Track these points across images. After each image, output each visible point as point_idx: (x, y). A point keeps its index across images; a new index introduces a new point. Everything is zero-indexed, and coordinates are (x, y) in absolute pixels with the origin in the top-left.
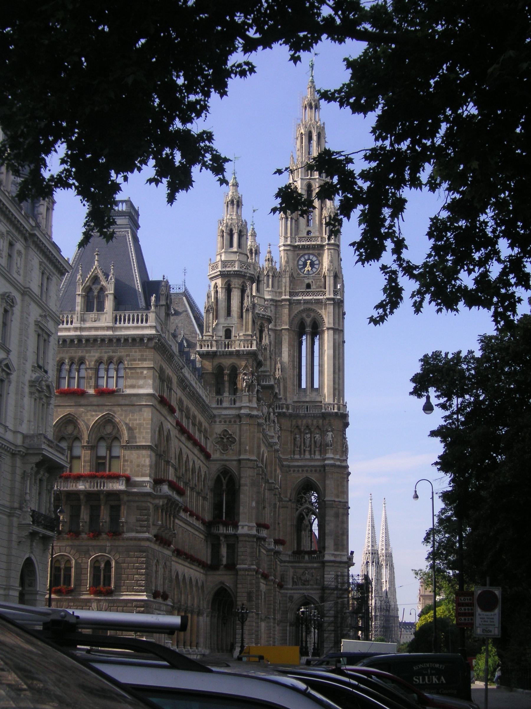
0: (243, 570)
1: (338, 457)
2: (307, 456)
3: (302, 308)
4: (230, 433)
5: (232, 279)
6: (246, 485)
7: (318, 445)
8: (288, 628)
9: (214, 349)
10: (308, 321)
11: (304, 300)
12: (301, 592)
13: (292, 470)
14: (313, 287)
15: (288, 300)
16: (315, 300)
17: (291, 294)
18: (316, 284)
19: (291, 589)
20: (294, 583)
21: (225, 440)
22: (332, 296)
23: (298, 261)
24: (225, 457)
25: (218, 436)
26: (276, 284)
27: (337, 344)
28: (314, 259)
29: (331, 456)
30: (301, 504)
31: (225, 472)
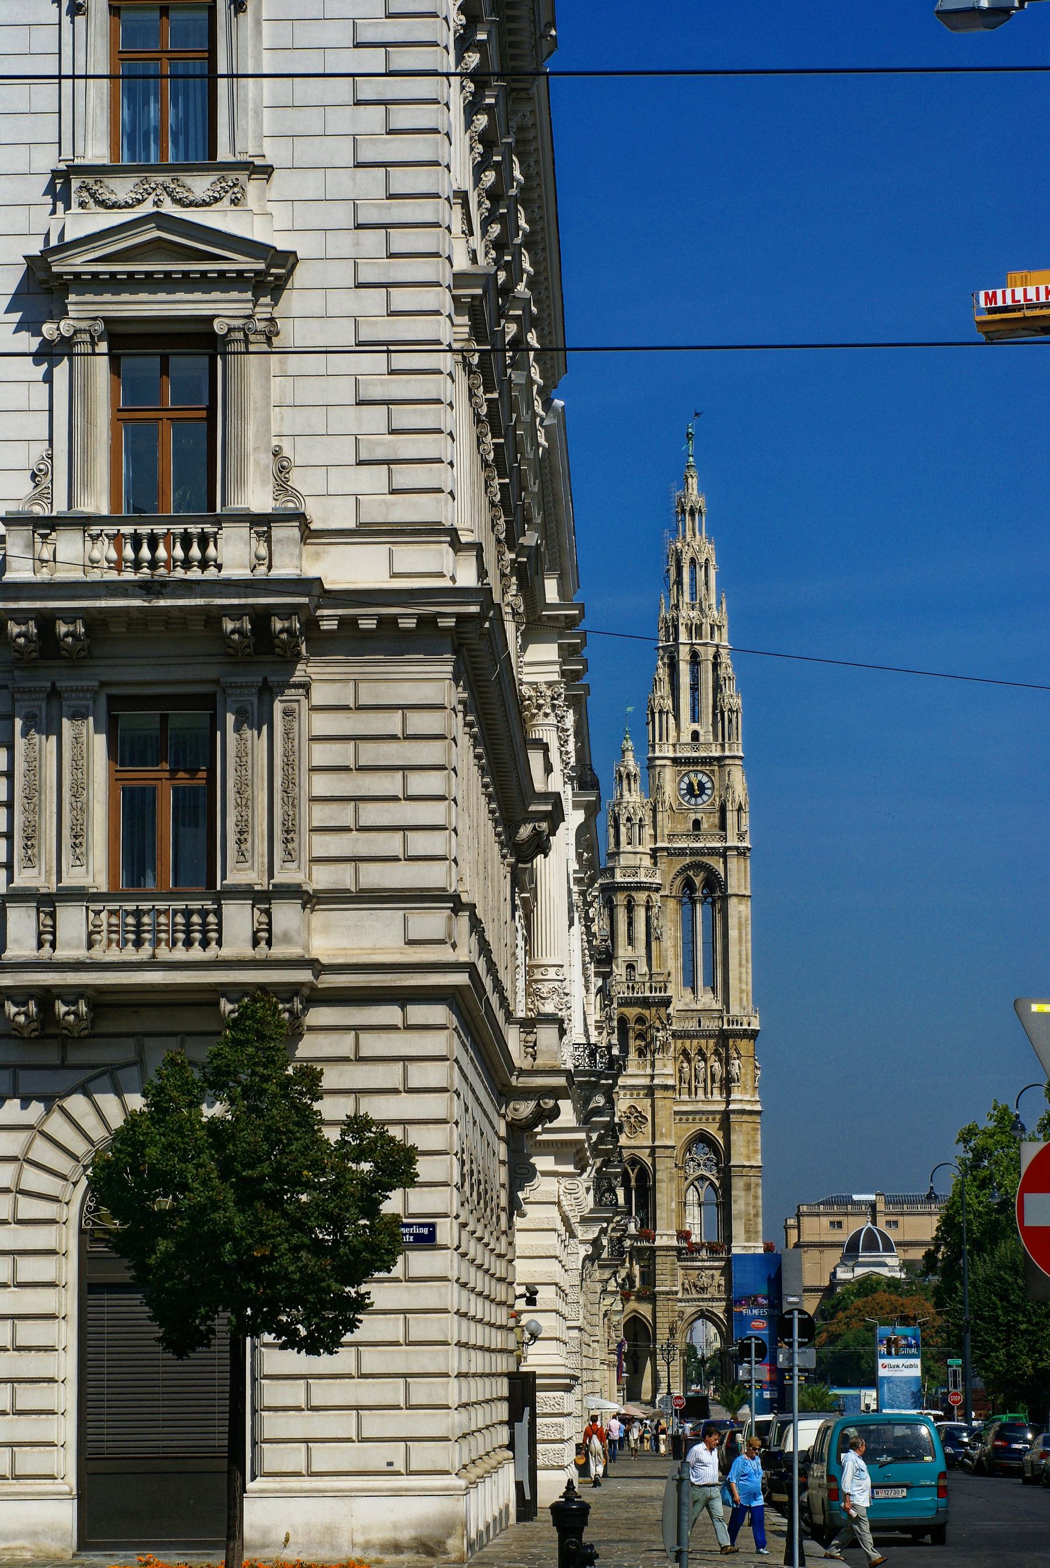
1: (747, 1098)
2: (701, 1095)
3: (688, 860)
5: (633, 894)
6: (662, 1181)
11: (691, 849)
14: (705, 826)
16: (708, 848)
18: (708, 822)
19: (680, 1301)
20: (685, 1290)
21: (632, 1120)
23: (679, 783)
27: (743, 920)
28: (705, 779)
29: (739, 1097)
31: (635, 1161)
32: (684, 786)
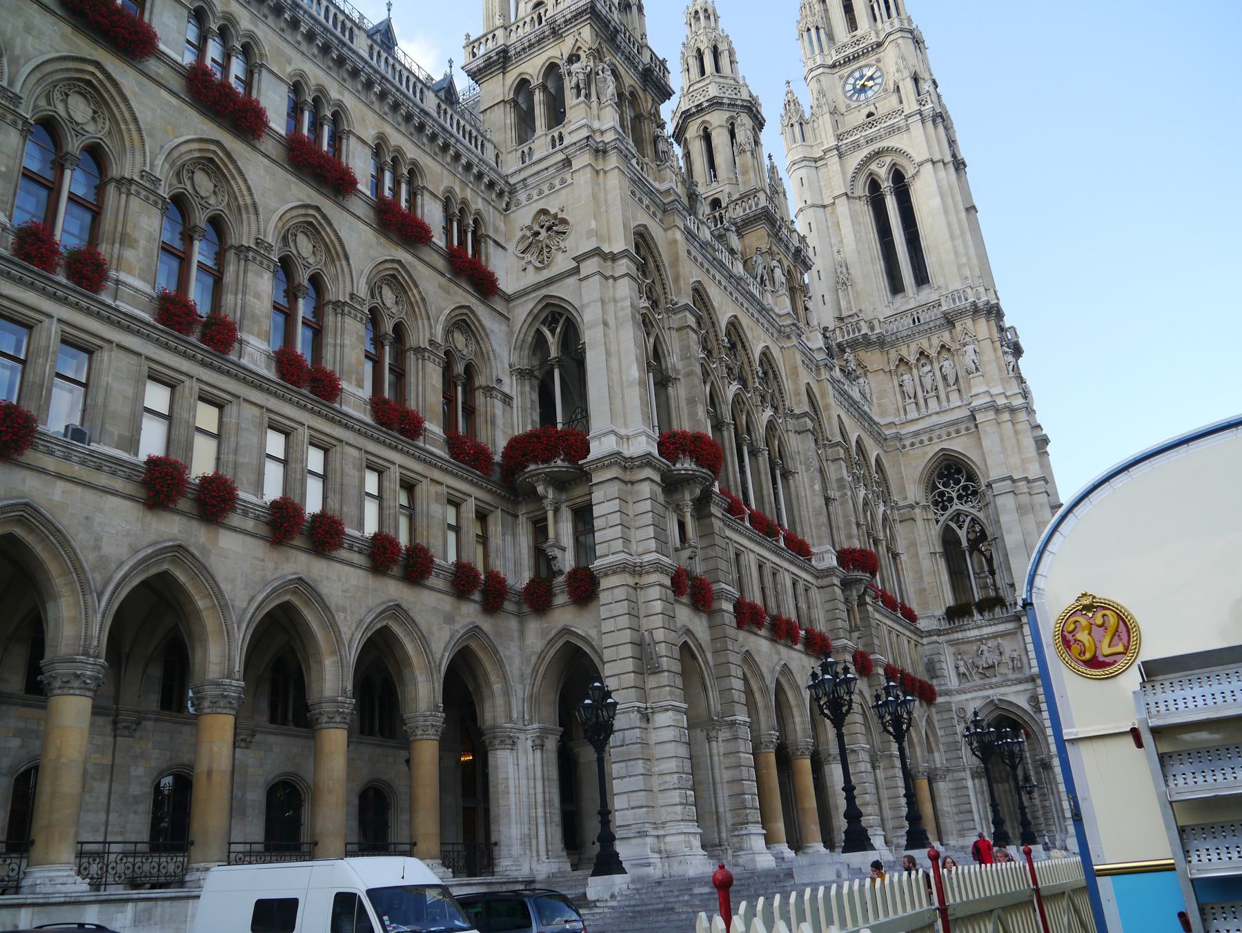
0: (615, 573)
4: (553, 211)
7: (951, 380)
8: (970, 783)
9: (501, 42)
10: (882, 171)
12: (985, 693)
13: (907, 443)
15: (838, 148)
17: (839, 137)
19: (959, 692)
20: (962, 676)
22: (916, 107)
24: (546, 274)
25: (529, 234)
26: (808, 135)
30: (944, 509)
32: (849, 87)
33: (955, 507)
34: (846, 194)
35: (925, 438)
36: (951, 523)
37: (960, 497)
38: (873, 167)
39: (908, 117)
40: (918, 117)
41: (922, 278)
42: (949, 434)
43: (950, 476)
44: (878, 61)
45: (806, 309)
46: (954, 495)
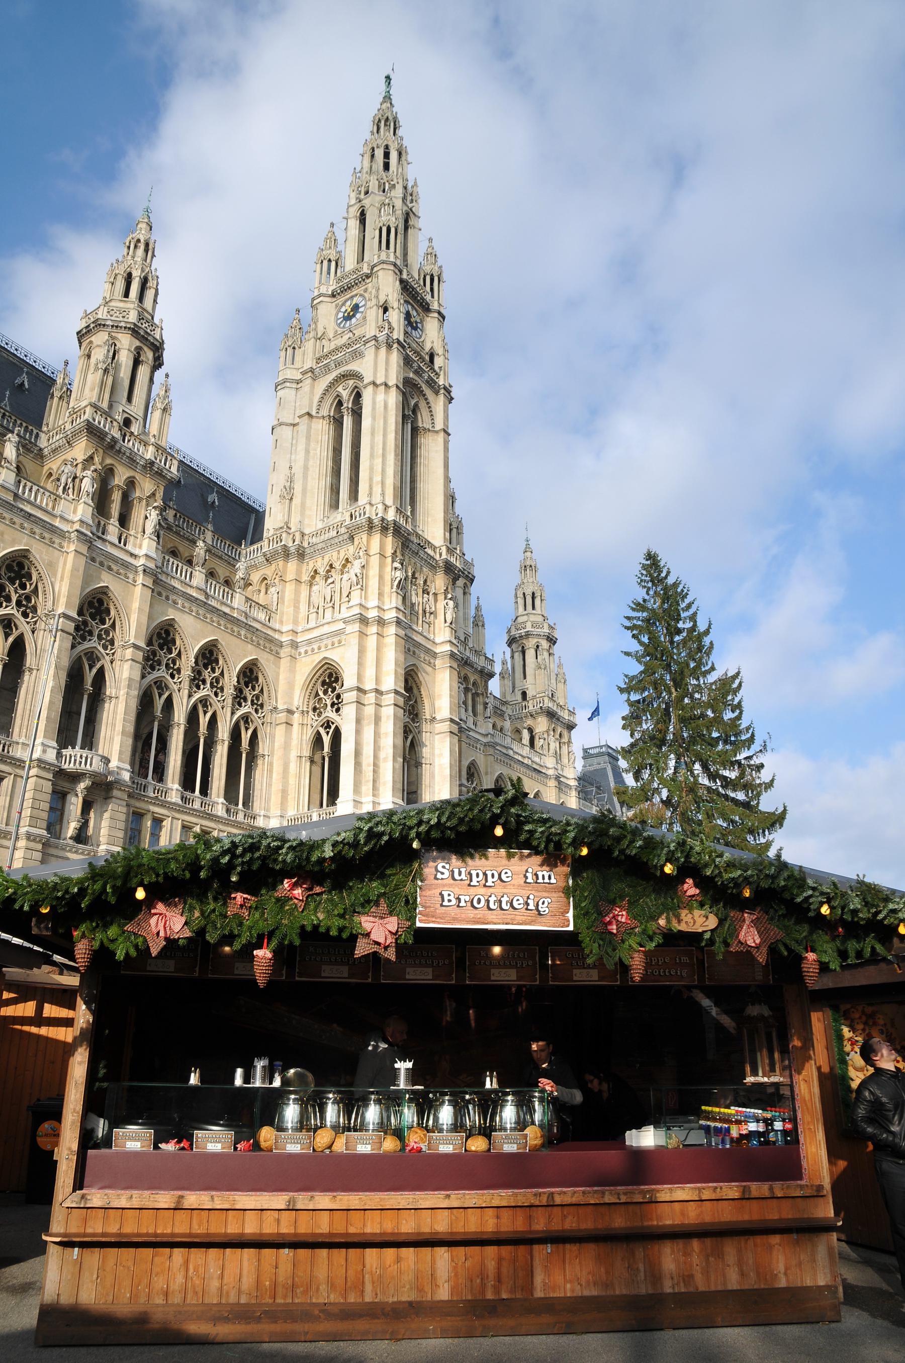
10: (345, 394)
17: (319, 360)
23: (337, 314)
30: (319, 715)
32: (341, 315)
33: (326, 714)
34: (308, 414)
35: (315, 646)
36: (322, 731)
37: (333, 705)
38: (340, 389)
39: (366, 342)
40: (373, 342)
41: (354, 495)
42: (333, 644)
43: (330, 685)
44: (366, 290)
45: (146, 518)
46: (329, 703)
